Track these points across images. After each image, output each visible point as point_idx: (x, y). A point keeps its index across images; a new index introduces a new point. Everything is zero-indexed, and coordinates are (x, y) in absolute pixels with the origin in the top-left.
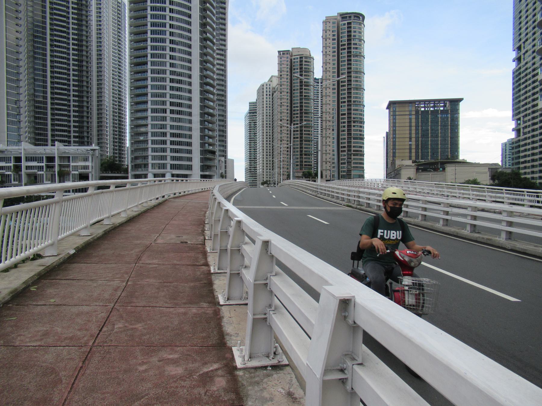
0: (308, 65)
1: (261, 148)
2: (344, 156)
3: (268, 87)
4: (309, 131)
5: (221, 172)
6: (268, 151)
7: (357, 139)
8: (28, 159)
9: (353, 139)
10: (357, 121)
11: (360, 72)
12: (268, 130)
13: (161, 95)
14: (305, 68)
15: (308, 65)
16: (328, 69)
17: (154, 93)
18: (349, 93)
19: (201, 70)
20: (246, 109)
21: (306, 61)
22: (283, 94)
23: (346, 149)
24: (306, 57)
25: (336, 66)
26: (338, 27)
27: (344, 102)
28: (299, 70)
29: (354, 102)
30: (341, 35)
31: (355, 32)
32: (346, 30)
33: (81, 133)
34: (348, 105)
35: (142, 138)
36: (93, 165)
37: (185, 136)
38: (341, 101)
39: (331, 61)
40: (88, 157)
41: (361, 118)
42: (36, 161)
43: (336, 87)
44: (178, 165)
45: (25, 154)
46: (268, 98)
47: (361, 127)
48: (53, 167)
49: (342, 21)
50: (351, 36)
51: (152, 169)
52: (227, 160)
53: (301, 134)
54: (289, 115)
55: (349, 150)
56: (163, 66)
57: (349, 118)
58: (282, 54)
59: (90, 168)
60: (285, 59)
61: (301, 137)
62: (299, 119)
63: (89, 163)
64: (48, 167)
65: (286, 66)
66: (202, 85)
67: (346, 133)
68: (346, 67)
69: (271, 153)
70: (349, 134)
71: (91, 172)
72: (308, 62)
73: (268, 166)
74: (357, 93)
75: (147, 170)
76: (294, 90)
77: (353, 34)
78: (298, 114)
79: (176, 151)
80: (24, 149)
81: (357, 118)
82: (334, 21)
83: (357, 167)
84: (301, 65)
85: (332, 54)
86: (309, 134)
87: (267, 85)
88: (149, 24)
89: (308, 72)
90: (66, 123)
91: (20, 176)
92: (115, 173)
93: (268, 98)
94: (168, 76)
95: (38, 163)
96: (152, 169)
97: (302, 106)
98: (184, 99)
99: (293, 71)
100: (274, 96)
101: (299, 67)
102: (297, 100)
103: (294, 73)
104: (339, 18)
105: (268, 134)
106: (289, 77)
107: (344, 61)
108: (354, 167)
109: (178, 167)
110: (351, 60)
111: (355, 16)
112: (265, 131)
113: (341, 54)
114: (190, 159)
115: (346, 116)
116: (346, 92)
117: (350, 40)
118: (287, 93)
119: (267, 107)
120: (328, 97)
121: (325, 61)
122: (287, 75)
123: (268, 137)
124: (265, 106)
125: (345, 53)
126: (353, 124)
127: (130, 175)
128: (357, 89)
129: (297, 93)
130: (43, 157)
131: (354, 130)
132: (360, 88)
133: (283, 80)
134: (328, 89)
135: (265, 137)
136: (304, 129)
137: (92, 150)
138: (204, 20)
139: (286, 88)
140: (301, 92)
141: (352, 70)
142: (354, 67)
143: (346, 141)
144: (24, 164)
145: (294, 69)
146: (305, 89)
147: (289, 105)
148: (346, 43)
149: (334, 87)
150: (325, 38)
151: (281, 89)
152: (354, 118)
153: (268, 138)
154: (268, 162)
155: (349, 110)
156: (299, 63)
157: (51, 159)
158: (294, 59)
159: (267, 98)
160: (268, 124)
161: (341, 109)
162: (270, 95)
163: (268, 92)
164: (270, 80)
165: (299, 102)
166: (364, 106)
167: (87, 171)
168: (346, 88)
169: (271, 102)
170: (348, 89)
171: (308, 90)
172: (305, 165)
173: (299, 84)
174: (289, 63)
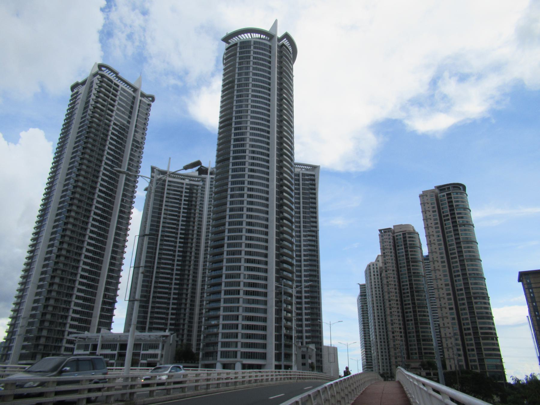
0: (413, 241)
1: (373, 334)
2: (471, 340)
3: (375, 267)
4: (424, 312)
5: (310, 361)
6: (382, 337)
7: (484, 319)
8: (104, 347)
9: (478, 319)
10: (479, 297)
11: (472, 242)
12: (380, 312)
13: (235, 276)
14: (410, 244)
15: (413, 241)
16: (432, 242)
17: (228, 274)
18: (463, 265)
19: (278, 249)
20: (358, 292)
21: (410, 237)
22: (388, 272)
23: (471, 331)
24: (410, 233)
25: (441, 238)
26: (437, 200)
27: (459, 276)
28: (403, 247)
29: (470, 274)
30: (441, 207)
31: (457, 201)
32: (446, 201)
33: (178, 320)
34: (463, 279)
35: (213, 322)
36: (164, 353)
38: (454, 274)
39: (434, 233)
40: (159, 344)
41: (483, 293)
42: (110, 348)
43: (445, 259)
44: (249, 352)
45: (102, 341)
46: (376, 279)
47: (485, 303)
49: (440, 193)
50: (453, 206)
51: (221, 357)
52: (323, 347)
53: (415, 316)
54: (398, 295)
55: (475, 333)
56: (239, 247)
57: (468, 293)
58: (384, 232)
59: (159, 356)
60: (387, 237)
61: (416, 320)
62: (410, 298)
63: (158, 352)
65: (388, 243)
66: (278, 264)
67: (467, 311)
68: (453, 238)
69: (386, 339)
70: (472, 313)
71: (159, 361)
72: (412, 237)
73: (384, 355)
74: (472, 265)
75: (216, 359)
76: (401, 267)
77: (454, 204)
78: (408, 293)
79: (249, 336)
80: (102, 336)
81: (478, 293)
82: (431, 194)
83: (491, 355)
84: (405, 241)
85: (434, 226)
86: (424, 316)
87: (373, 265)
89: (414, 247)
90: (165, 311)
92: (188, 363)
93: (376, 279)
94: (243, 256)
95: (112, 350)
96: (221, 357)
97: (412, 284)
98: (260, 280)
99: (397, 248)
100: (382, 275)
101: (403, 243)
102: (405, 279)
103: (398, 250)
104: (437, 191)
105: (380, 317)
106: (393, 254)
107: (450, 232)
108: (486, 355)
109: (249, 356)
110: (457, 230)
111: (454, 187)
112: (376, 314)
113: (445, 225)
114: (264, 346)
115: (464, 292)
116: (458, 264)
117: (453, 210)
118: (393, 271)
119: (376, 288)
120: (437, 271)
121: (427, 234)
122: (391, 252)
123: (380, 320)
124: (373, 286)
125: (449, 224)
126: (474, 301)
127: (200, 365)
128: (471, 260)
129: (404, 270)
130: (117, 344)
131: (477, 308)
132: (475, 259)
133: (387, 258)
134: (436, 263)
135: (377, 321)
136: (417, 309)
137: (164, 336)
138: (281, 202)
139: (391, 265)
140: (409, 269)
141: (461, 240)
142: (462, 237)
143: (469, 321)
145: (398, 246)
146: (413, 266)
147: (397, 283)
148: (449, 213)
149: (442, 260)
150: (424, 212)
151: (386, 267)
152: (474, 293)
153: (381, 322)
154: (383, 351)
155: (466, 284)
156: (402, 240)
158: (397, 236)
159: (375, 278)
160: (379, 306)
161: (455, 283)
162: (377, 275)
163: (376, 272)
164: (377, 260)
165: (407, 279)
166: (485, 279)
167: (156, 360)
168: (457, 260)
169: (380, 282)
170: (460, 261)
171: (417, 266)
172: (426, 353)
173: (405, 261)
174: (392, 241)
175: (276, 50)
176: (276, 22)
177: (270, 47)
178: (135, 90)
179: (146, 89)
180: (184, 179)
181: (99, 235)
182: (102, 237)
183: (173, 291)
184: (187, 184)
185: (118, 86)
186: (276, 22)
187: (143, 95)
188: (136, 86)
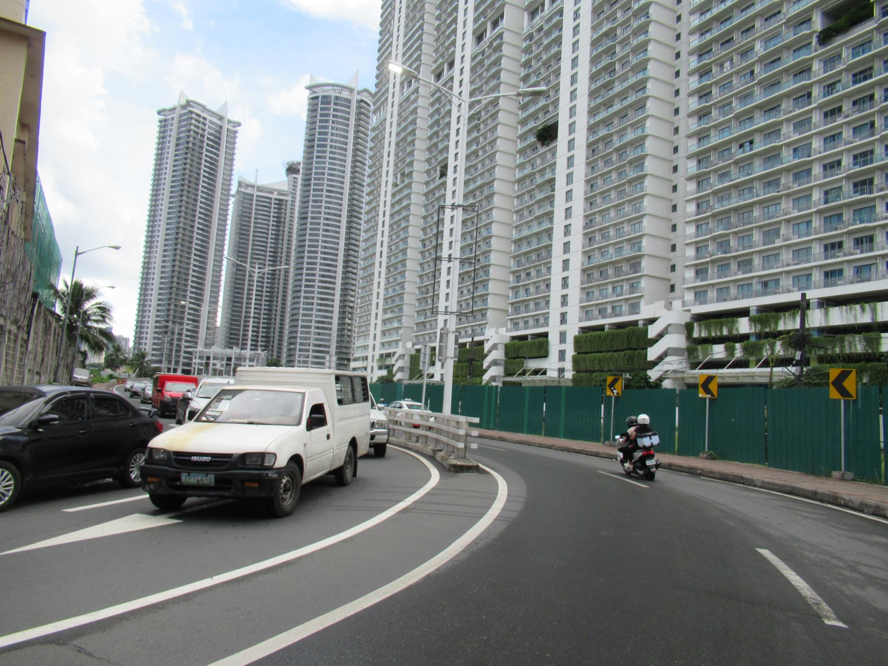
8: (214, 358)
37: (325, 346)
48: (230, 365)
64: (227, 365)
88: (305, 263)
91: (208, 370)
144: (212, 361)
157: (229, 359)
175: (354, 105)
176: (358, 71)
177: (349, 101)
178: (221, 118)
179: (233, 116)
180: (272, 193)
181: (200, 267)
182: (202, 268)
183: (263, 307)
184: (276, 199)
185: (205, 119)
186: (358, 71)
187: (229, 122)
188: (222, 114)
